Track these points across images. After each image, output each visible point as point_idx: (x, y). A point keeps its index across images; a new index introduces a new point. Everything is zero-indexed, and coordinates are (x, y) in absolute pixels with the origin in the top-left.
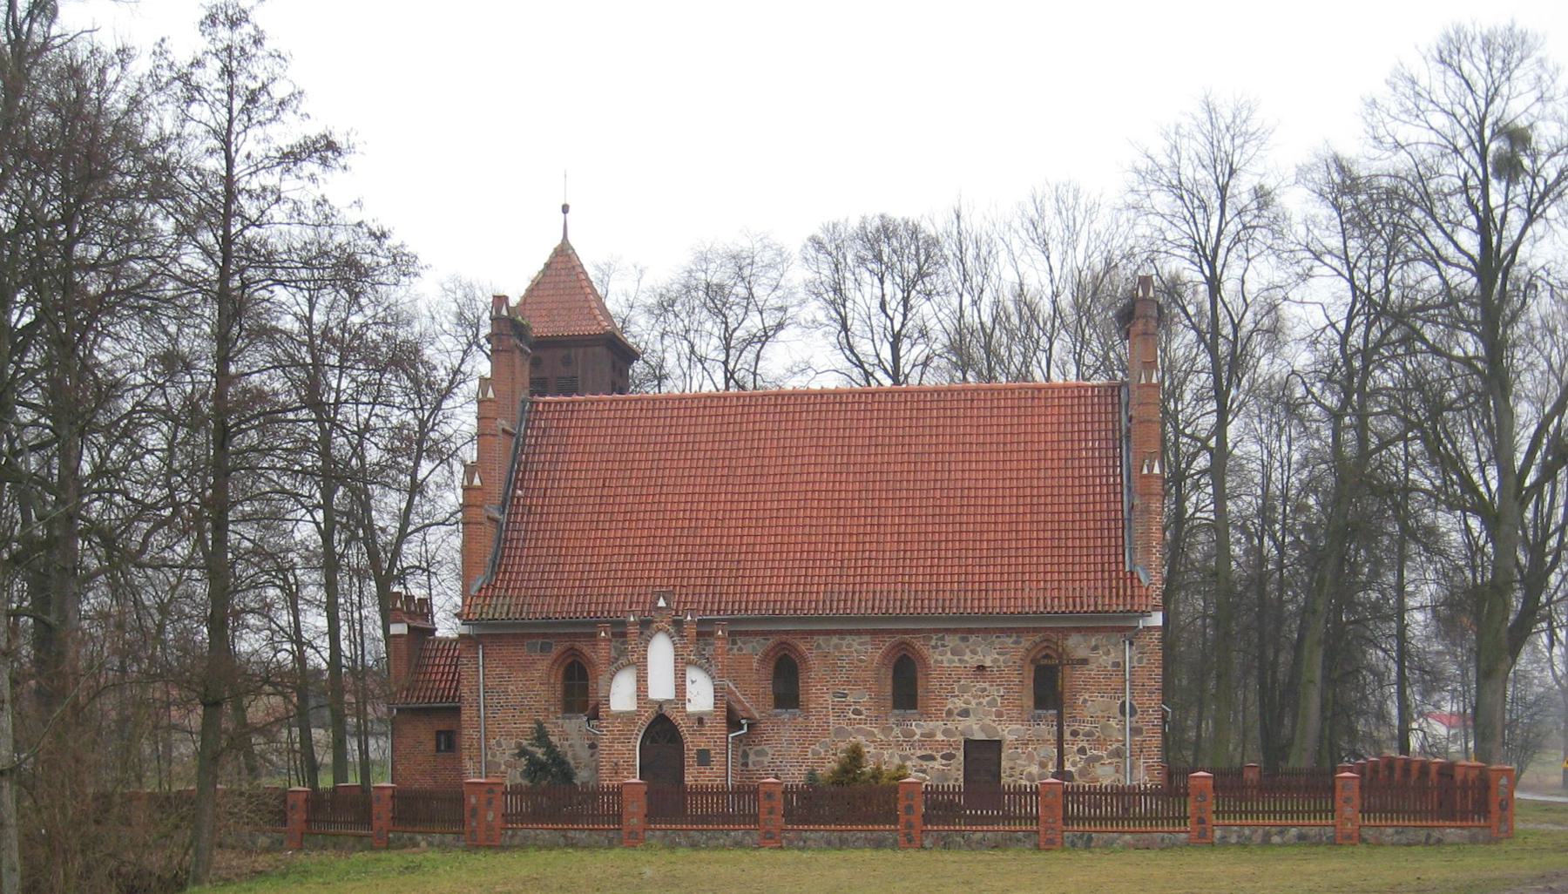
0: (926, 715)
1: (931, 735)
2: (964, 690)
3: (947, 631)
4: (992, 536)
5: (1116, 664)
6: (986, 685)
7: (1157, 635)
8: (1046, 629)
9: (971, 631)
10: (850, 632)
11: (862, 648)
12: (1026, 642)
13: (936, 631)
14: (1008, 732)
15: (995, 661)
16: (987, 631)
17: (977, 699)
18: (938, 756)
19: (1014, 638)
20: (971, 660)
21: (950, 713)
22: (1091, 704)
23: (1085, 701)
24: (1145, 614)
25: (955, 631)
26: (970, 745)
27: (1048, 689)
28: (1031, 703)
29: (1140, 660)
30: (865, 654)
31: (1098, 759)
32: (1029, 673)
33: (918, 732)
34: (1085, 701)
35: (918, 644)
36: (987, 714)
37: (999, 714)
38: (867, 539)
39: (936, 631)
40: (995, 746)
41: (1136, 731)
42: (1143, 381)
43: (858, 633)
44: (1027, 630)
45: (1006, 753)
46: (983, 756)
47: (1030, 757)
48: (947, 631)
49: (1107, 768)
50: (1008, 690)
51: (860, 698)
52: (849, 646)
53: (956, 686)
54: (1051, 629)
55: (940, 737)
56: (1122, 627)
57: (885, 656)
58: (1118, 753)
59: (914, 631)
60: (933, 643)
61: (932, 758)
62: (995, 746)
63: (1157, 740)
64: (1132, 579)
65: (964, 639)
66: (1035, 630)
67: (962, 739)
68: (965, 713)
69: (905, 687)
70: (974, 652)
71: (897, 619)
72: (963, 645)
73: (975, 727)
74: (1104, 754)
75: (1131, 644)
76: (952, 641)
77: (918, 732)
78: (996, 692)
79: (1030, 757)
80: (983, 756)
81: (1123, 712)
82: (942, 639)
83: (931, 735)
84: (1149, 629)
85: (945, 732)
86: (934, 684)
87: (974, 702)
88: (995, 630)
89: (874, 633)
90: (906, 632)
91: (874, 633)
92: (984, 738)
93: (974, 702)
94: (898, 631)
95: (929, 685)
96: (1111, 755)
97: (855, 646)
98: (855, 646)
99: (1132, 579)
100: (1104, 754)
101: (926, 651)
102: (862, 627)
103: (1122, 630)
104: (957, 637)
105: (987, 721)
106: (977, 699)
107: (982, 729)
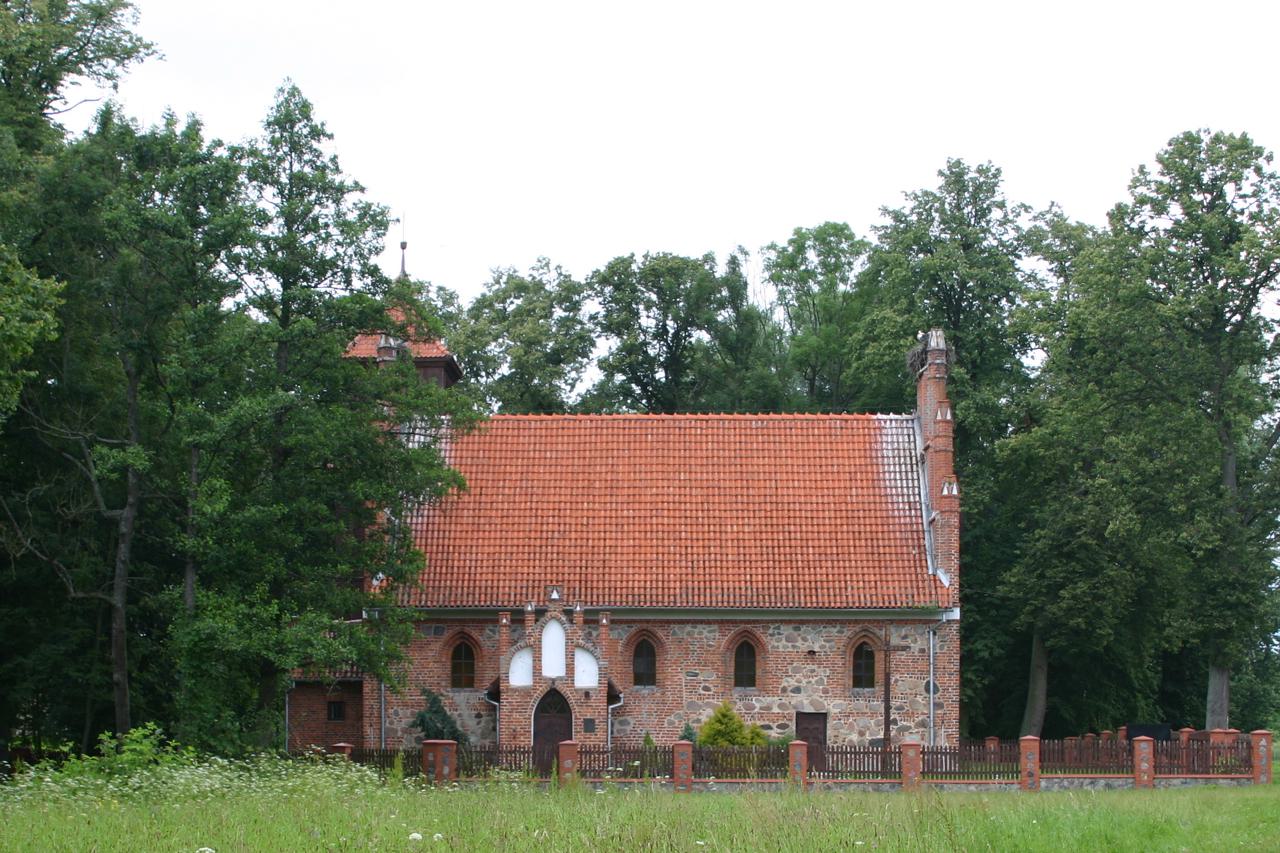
0: (766, 692)
1: (768, 708)
2: (797, 670)
3: (782, 621)
4: (816, 543)
5: (922, 651)
6: (815, 667)
7: (956, 626)
8: (864, 621)
9: (803, 622)
10: (701, 622)
11: (711, 635)
12: (848, 632)
13: (773, 622)
14: (833, 706)
15: (822, 647)
16: (815, 622)
17: (805, 679)
18: (774, 726)
19: (838, 628)
20: (803, 646)
21: (784, 690)
22: (904, 684)
23: (896, 681)
24: (947, 609)
25: (789, 622)
26: (801, 717)
27: (864, 669)
28: (851, 683)
29: (941, 648)
30: (714, 640)
31: (908, 728)
32: (850, 658)
33: (758, 705)
34: (896, 681)
35: (759, 631)
36: (815, 691)
37: (825, 691)
38: (712, 543)
39: (773, 622)
40: (822, 717)
41: (938, 706)
42: (939, 417)
43: (709, 622)
44: (849, 622)
45: (831, 723)
46: (812, 724)
47: (851, 727)
48: (782, 621)
49: (914, 736)
50: (833, 671)
51: (709, 676)
52: (700, 633)
53: (790, 668)
54: (869, 621)
55: (776, 710)
56: (924, 618)
57: (731, 642)
58: (923, 724)
59: (754, 622)
60: (771, 631)
61: (769, 727)
62: (822, 717)
63: (955, 713)
64: (935, 581)
65: (797, 629)
66: (856, 622)
67: (794, 712)
68: (797, 690)
69: (746, 666)
70: (805, 640)
71: (743, 612)
72: (796, 634)
73: (806, 702)
74: (912, 724)
75: (935, 634)
76: (786, 630)
77: (758, 705)
78: (823, 673)
79: (851, 727)
80: (812, 724)
81: (927, 690)
82: (779, 628)
83: (768, 708)
84: (949, 621)
85: (780, 706)
86: (771, 666)
87: (804, 681)
88: (822, 621)
89: (721, 622)
90: (748, 622)
91: (721, 622)
92: (813, 711)
93: (804, 681)
94: (742, 622)
95: (766, 666)
96: (918, 725)
97: (705, 633)
98: (705, 633)
99: (935, 581)
100: (912, 724)
101: (765, 639)
102: (711, 617)
103: (927, 622)
104: (791, 626)
105: (815, 697)
106: (805, 679)
107: (811, 703)
